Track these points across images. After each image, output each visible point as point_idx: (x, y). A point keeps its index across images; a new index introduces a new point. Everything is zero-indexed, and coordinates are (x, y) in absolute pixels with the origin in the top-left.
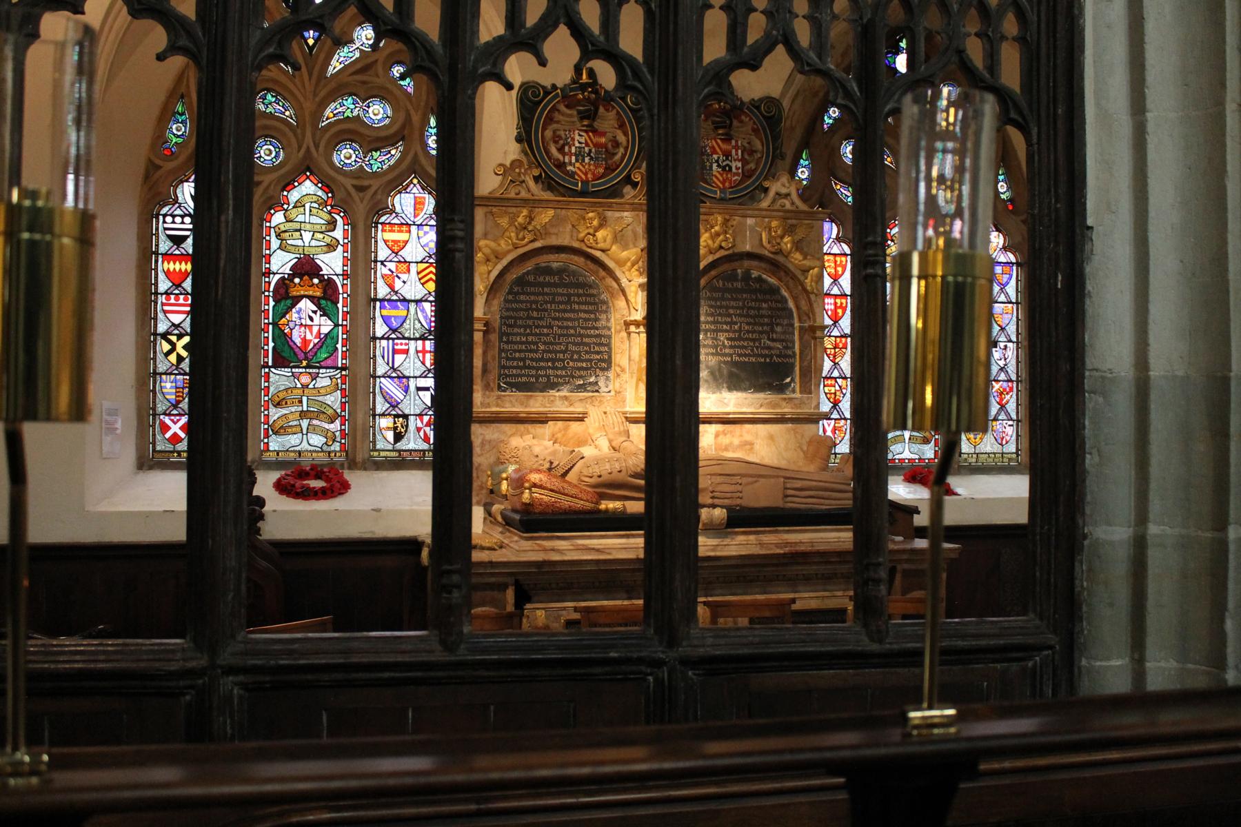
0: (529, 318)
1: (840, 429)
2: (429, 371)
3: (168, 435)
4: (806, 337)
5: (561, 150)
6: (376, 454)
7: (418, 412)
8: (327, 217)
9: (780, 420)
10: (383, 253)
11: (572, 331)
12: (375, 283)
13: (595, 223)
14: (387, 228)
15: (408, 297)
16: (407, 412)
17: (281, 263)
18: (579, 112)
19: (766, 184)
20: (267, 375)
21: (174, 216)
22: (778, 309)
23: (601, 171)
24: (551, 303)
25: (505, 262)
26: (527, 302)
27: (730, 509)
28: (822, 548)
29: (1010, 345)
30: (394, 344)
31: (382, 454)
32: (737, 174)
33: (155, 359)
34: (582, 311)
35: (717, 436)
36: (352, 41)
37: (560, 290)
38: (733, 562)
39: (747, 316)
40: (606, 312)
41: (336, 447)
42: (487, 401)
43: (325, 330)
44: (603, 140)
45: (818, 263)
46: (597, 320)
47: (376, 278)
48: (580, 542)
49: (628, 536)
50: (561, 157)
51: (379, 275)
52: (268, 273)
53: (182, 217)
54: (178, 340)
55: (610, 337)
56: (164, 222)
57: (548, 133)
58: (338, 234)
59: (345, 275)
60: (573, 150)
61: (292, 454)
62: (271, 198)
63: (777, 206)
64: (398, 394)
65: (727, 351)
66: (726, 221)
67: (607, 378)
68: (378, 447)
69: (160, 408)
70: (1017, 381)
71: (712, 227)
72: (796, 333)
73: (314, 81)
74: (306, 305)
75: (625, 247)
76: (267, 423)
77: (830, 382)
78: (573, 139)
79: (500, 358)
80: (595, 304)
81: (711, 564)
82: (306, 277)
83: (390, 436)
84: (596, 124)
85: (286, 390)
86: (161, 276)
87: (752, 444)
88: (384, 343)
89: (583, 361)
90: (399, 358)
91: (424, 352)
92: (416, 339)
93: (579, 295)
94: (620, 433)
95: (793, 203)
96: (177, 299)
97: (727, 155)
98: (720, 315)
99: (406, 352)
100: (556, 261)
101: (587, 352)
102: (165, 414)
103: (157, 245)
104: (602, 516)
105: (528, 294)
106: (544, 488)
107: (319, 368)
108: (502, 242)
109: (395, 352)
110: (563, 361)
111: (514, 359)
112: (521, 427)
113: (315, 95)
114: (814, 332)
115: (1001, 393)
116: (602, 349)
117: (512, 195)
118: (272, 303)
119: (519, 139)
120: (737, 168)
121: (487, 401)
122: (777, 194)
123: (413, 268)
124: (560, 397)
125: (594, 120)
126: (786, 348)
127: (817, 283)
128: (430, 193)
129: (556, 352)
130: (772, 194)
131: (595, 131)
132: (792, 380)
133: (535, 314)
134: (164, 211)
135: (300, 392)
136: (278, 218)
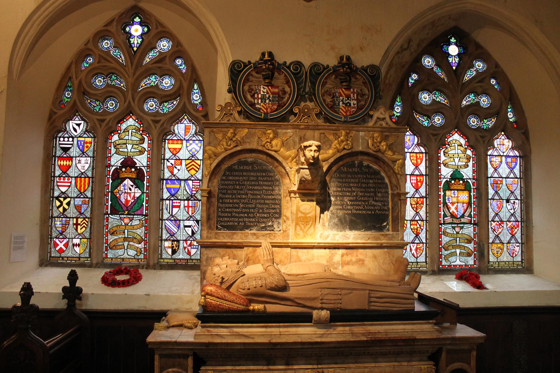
0: (234, 189)
1: (420, 248)
2: (191, 217)
3: (58, 248)
4: (396, 199)
5: (253, 96)
6: (162, 260)
7: (185, 238)
8: (140, 137)
9: (380, 247)
10: (168, 155)
11: (259, 197)
12: (164, 170)
13: (271, 136)
14: (171, 142)
15: (180, 178)
16: (179, 238)
17: (116, 160)
18: (263, 75)
19: (371, 113)
20: (107, 219)
21: (64, 138)
22: (379, 183)
23: (276, 107)
24: (247, 181)
25: (220, 158)
26: (233, 180)
27: (332, 311)
28: (392, 336)
29: (517, 201)
30: (172, 203)
31: (165, 261)
32: (353, 108)
33: (52, 210)
34: (264, 185)
35: (342, 256)
36: (155, 48)
37: (252, 174)
38: (332, 345)
39: (361, 187)
40: (278, 186)
41: (142, 256)
42: (210, 235)
43: (137, 195)
44: (277, 90)
45: (401, 157)
46: (273, 190)
47: (164, 168)
48: (236, 330)
49: (266, 327)
50: (253, 100)
51: (165, 166)
52: (109, 166)
53: (68, 138)
54: (64, 200)
55: (280, 200)
56: (59, 141)
57: (246, 88)
58: (145, 145)
59: (148, 166)
60: (260, 96)
62: (110, 127)
63: (378, 125)
64: (175, 229)
65: (349, 207)
66: (347, 134)
67: (279, 223)
68: (163, 257)
69: (54, 235)
70: (521, 222)
71: (339, 137)
72: (390, 197)
73: (134, 66)
74: (128, 182)
75: (288, 149)
76: (107, 243)
77: (414, 223)
78: (260, 90)
79: (218, 211)
80: (272, 181)
81: (318, 346)
82: (128, 168)
83: (170, 251)
84: (273, 82)
85: (117, 226)
86: (57, 168)
87: (363, 261)
88: (168, 202)
89: (265, 213)
90: (175, 210)
91: (188, 207)
92: (184, 200)
93: (263, 177)
94: (267, 260)
95: (387, 123)
96: (64, 179)
97: (348, 97)
98: (345, 187)
99: (179, 207)
100: (250, 157)
101: (267, 208)
102: (56, 238)
103: (55, 152)
104: (250, 314)
105: (234, 176)
106: (213, 296)
107: (134, 215)
108: (219, 148)
109: (173, 207)
110: (253, 213)
111: (226, 212)
112: (229, 250)
113: (134, 74)
114: (401, 197)
115: (512, 228)
116: (276, 206)
117: (226, 122)
118: (111, 181)
119: (229, 91)
120: (354, 104)
121: (210, 235)
122: (378, 118)
123: (184, 163)
124: (251, 233)
125: (272, 79)
126: (384, 205)
127: (401, 168)
128: (193, 123)
129: (249, 208)
130: (375, 118)
131: (272, 86)
132: (388, 224)
133: (238, 187)
134: (60, 135)
135: (124, 227)
136: (115, 138)
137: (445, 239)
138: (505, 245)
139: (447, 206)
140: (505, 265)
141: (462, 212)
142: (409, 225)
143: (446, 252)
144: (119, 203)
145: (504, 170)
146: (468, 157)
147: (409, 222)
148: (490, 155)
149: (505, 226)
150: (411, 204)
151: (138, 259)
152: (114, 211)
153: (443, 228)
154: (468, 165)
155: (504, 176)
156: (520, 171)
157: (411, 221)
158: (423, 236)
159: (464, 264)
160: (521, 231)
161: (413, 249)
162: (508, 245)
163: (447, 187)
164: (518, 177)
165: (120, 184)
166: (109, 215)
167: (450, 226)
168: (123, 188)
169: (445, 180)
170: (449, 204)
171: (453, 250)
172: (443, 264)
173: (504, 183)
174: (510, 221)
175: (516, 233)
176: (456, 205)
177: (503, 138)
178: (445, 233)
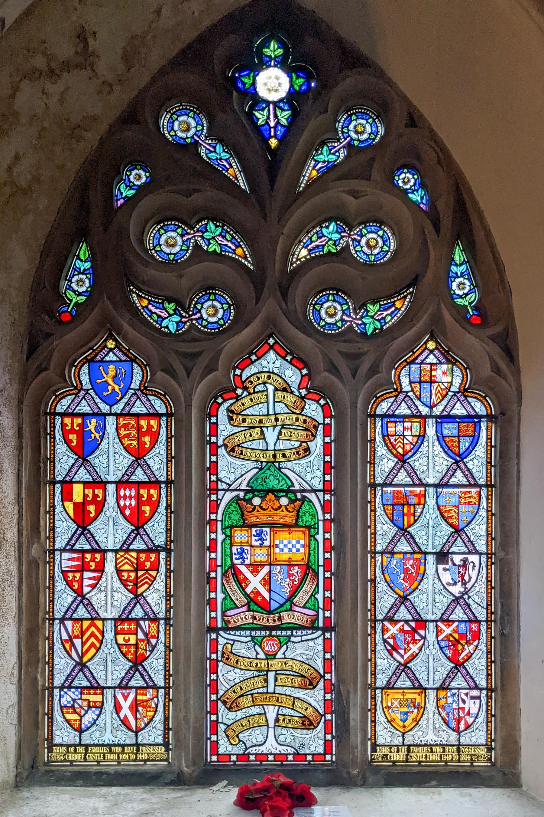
1: (145, 704)
29: (473, 558)
77: (126, 627)
115: (458, 641)
137: (228, 677)
138: (431, 694)
139: (236, 573)
140: (432, 757)
141: (287, 591)
142: (109, 635)
143: (232, 715)
145: (432, 461)
146: (310, 425)
147: (110, 625)
148: (383, 416)
149: (431, 637)
150: (119, 572)
153: (221, 641)
154: (307, 450)
155: (431, 481)
156: (489, 463)
157: (118, 620)
158: (155, 664)
159: (291, 750)
160: (489, 652)
161: (125, 705)
162: (442, 694)
163: (236, 517)
164: (482, 481)
167: (244, 636)
169: (229, 496)
170: (243, 569)
171: (255, 710)
172: (221, 750)
173: (431, 501)
174: (448, 622)
175: (469, 656)
176: (266, 569)
177: (431, 359)
178: (228, 657)
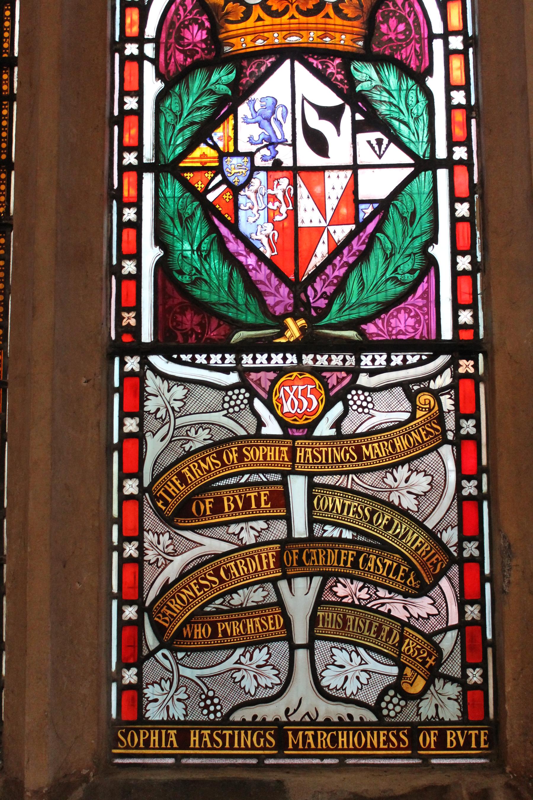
41: (444, 703)
43: (376, 185)
61: (251, 739)
76: (132, 594)
85: (217, 447)
107: (357, 348)
118: (152, 86)
135: (276, 454)
144: (229, 257)
151: (414, 730)
152: (190, 324)
165: (225, 108)
166: (144, 352)
168: (255, 131)
